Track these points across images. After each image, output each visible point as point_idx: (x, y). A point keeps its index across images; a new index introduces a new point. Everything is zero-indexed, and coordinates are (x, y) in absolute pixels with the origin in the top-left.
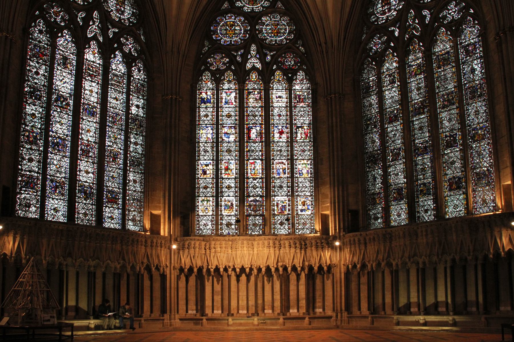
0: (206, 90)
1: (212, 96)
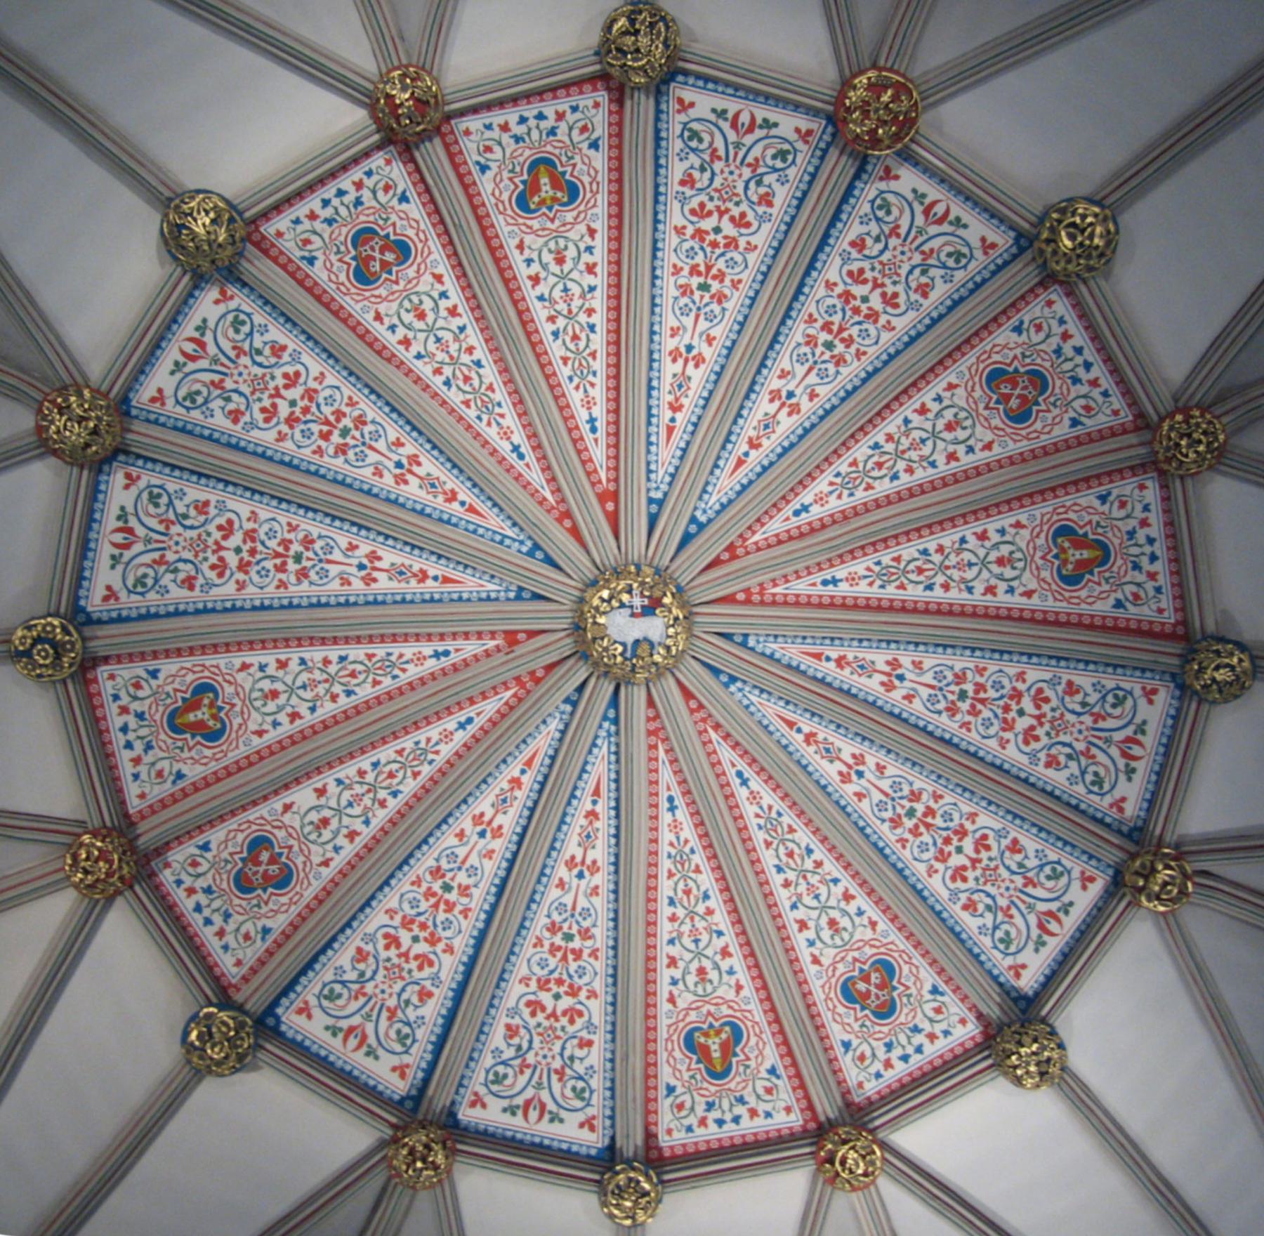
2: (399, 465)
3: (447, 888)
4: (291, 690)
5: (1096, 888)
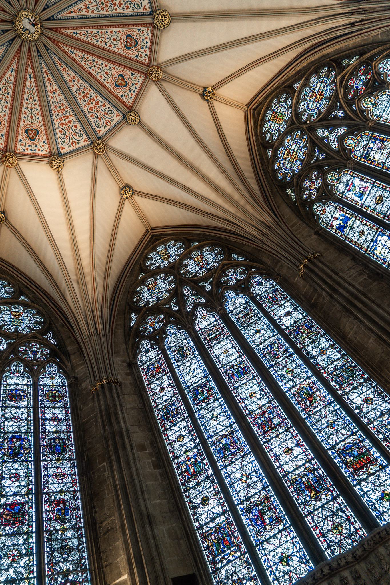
0: (332, 216)
1: (342, 213)
5: (86, 143)
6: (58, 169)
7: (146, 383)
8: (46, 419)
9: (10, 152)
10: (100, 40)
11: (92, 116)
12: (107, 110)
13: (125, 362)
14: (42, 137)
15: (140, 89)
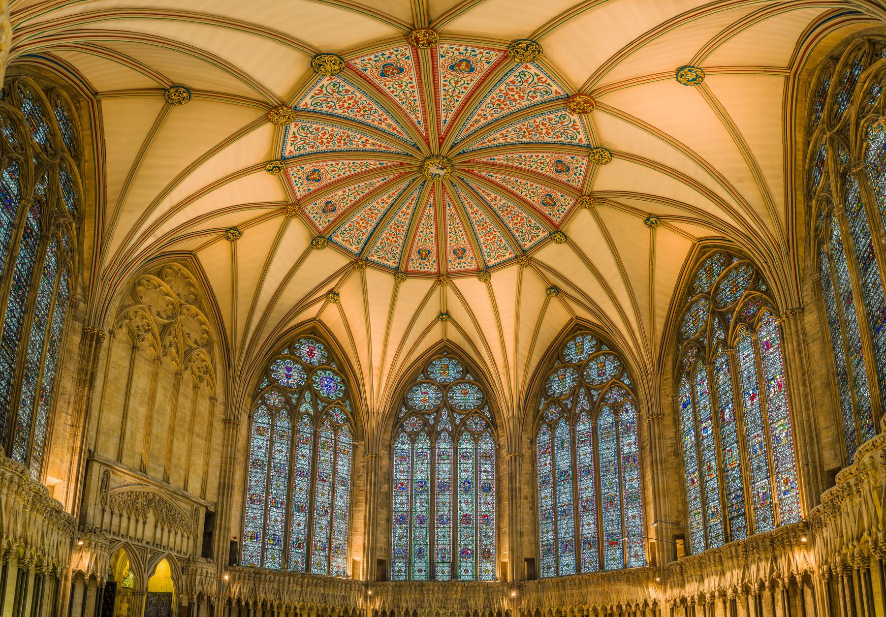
2: (380, 120)
3: (372, 213)
4: (339, 170)
6: (487, 281)
7: (538, 457)
8: (481, 472)
9: (442, 276)
10: (524, 163)
11: (517, 231)
12: (533, 225)
13: (529, 438)
14: (469, 254)
15: (571, 210)
